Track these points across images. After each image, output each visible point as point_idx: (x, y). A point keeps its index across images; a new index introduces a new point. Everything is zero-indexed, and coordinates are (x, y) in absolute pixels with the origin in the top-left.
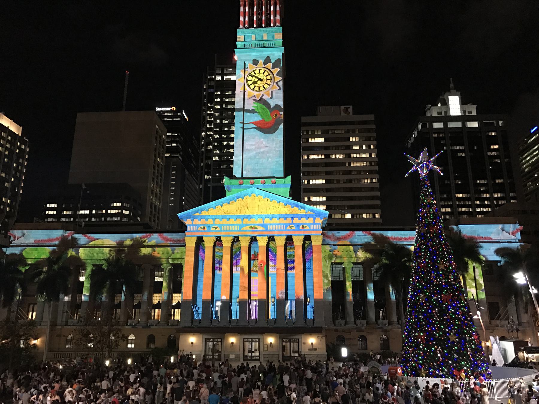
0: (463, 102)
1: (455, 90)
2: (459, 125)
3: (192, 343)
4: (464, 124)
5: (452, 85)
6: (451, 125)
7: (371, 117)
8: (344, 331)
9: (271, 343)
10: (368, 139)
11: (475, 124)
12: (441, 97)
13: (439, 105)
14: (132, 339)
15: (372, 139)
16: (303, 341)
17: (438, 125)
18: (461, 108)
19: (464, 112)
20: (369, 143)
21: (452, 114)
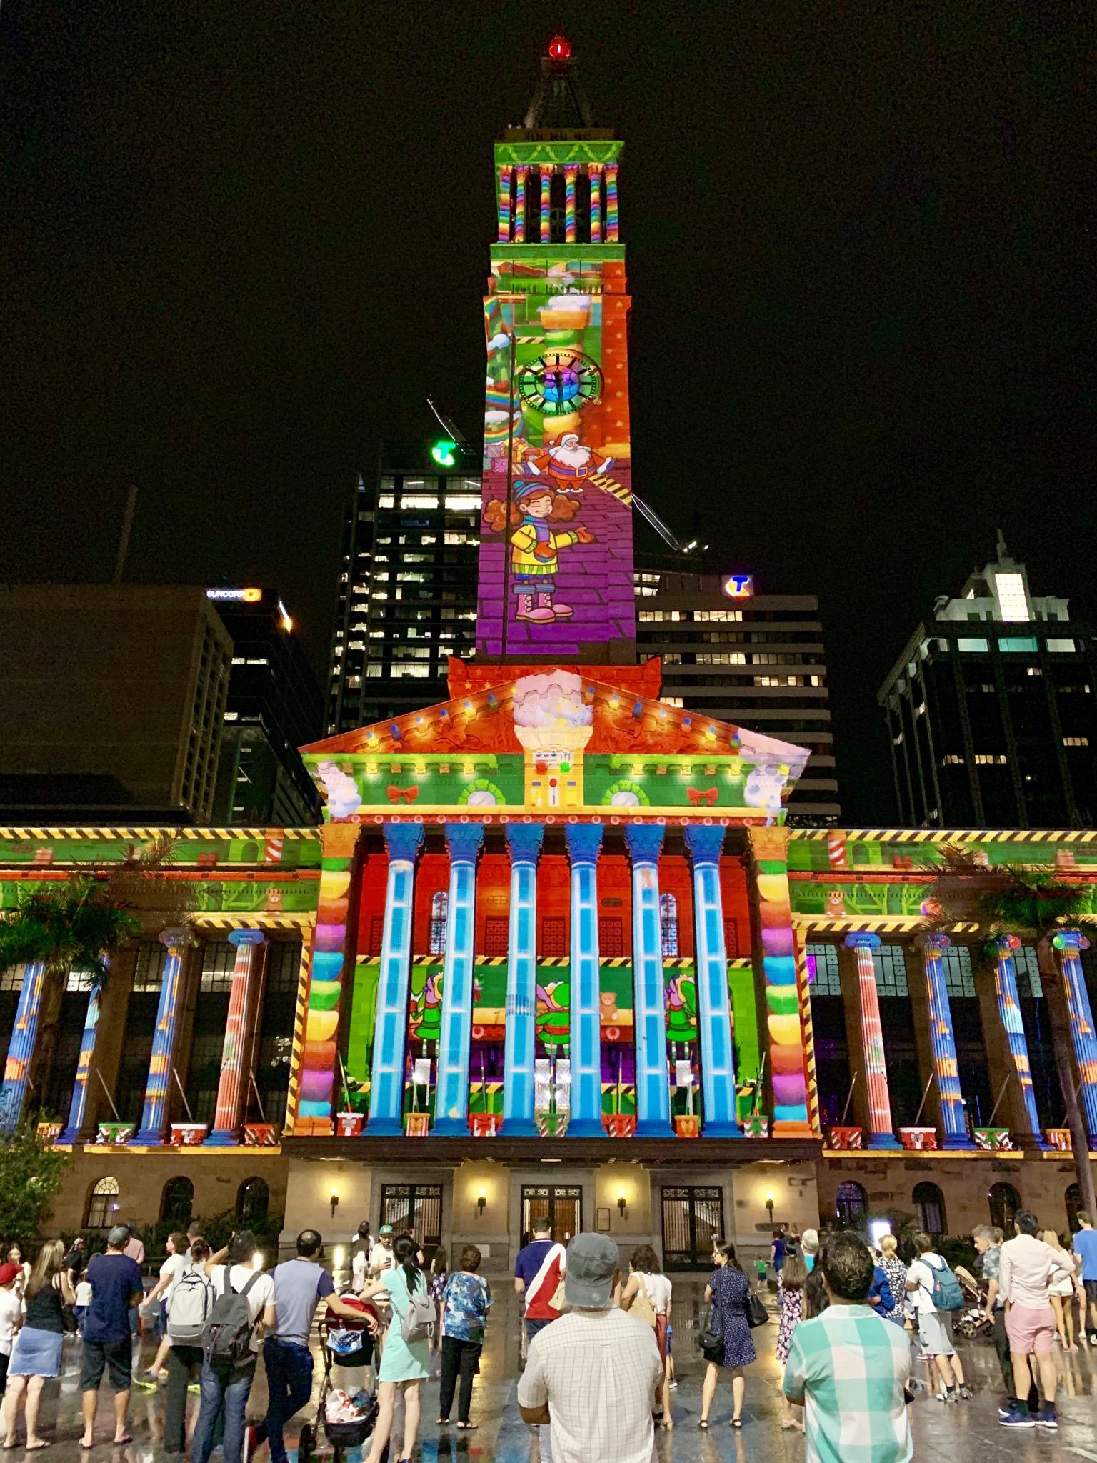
0: (1034, 589)
1: (1011, 561)
2: (1026, 645)
3: (335, 1201)
4: (1042, 646)
5: (1001, 547)
6: (1006, 645)
7: (810, 603)
8: (861, 1164)
9: (622, 1203)
10: (806, 660)
11: (1068, 646)
12: (974, 577)
13: (971, 596)
14: (108, 1198)
15: (813, 661)
16: (737, 1197)
17: (966, 645)
18: (1031, 607)
19: (1038, 614)
20: (806, 669)
21: (1005, 619)
